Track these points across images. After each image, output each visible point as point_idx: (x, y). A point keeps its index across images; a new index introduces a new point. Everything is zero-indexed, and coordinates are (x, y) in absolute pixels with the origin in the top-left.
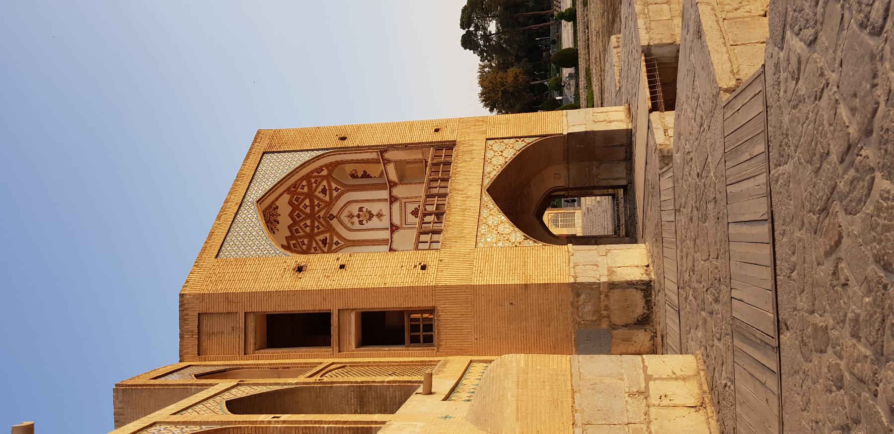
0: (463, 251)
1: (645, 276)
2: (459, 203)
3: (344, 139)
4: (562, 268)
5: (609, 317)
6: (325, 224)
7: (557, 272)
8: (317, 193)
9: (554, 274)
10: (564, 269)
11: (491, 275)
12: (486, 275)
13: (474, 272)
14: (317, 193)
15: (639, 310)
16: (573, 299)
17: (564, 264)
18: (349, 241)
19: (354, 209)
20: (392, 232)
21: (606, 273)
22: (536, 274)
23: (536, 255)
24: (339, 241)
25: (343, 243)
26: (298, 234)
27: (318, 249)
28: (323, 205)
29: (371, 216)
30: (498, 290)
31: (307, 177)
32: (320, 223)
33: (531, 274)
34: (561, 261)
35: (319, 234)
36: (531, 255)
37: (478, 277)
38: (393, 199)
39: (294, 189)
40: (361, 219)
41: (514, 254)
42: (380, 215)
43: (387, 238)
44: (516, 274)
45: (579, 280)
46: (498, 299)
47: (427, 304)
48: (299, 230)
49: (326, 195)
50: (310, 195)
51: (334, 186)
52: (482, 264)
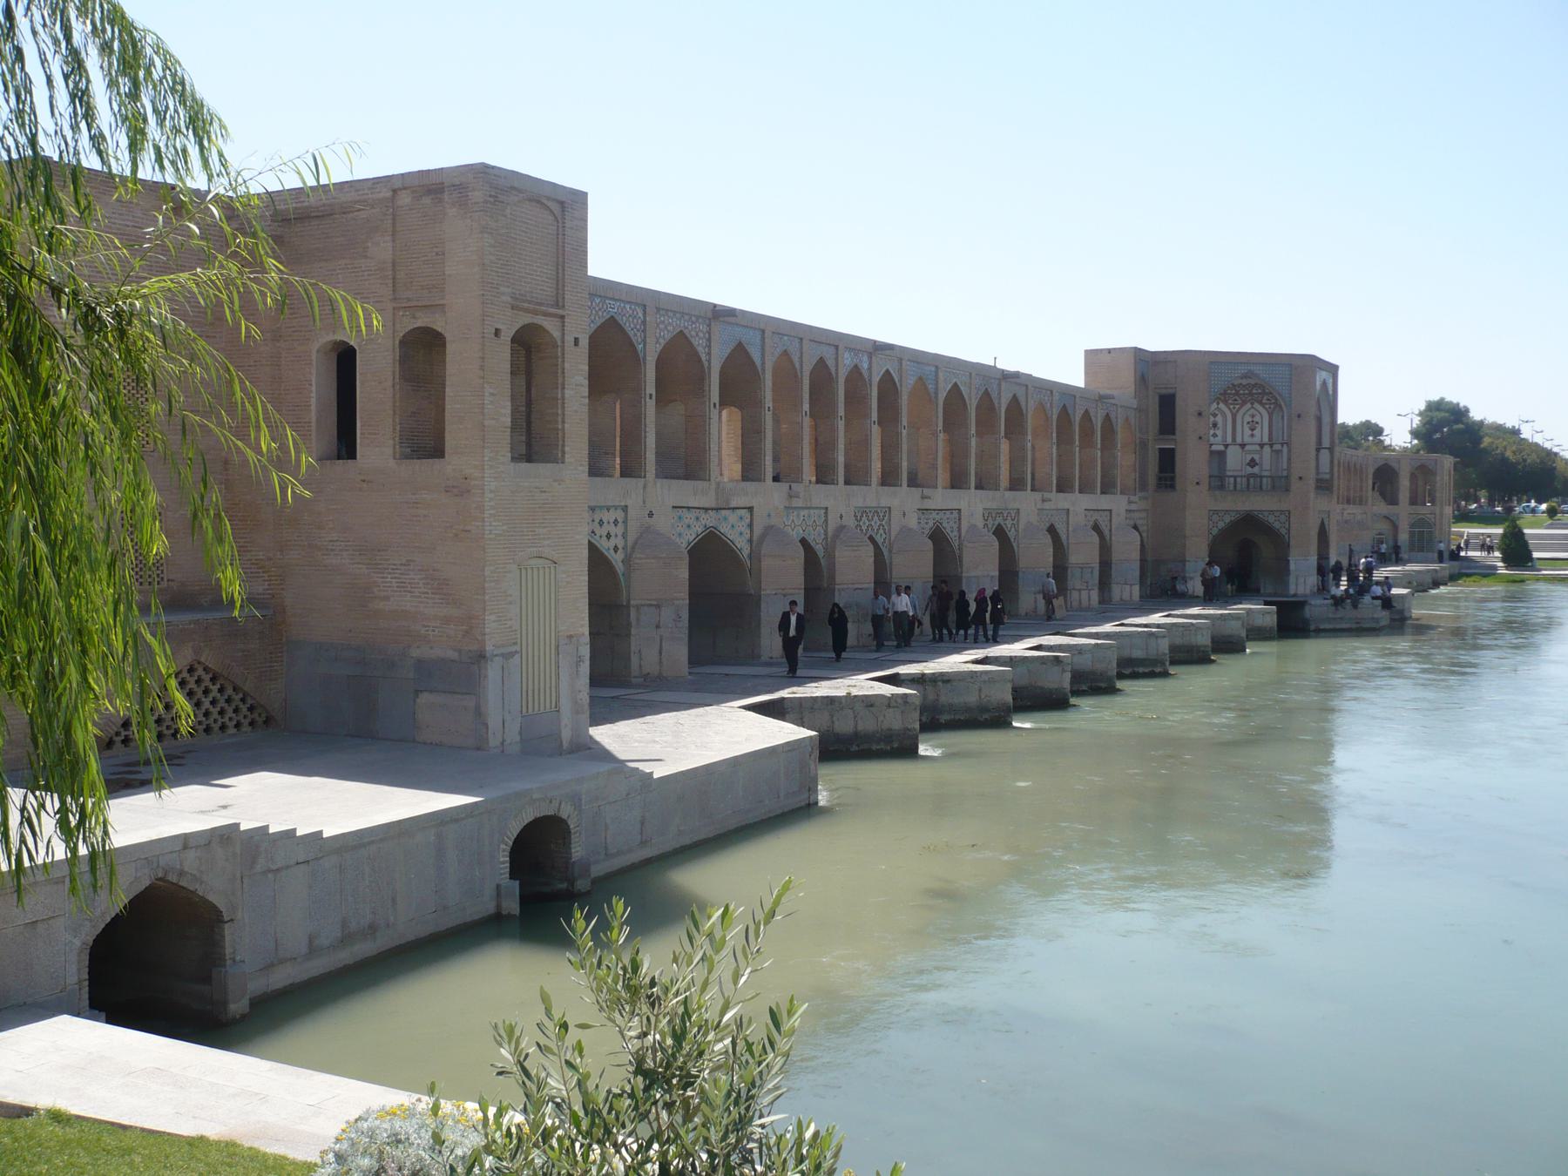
19: (1257, 419)
20: (1240, 445)
29: (1253, 430)
45: (1187, 563)
47: (1178, 486)
51: (1272, 406)
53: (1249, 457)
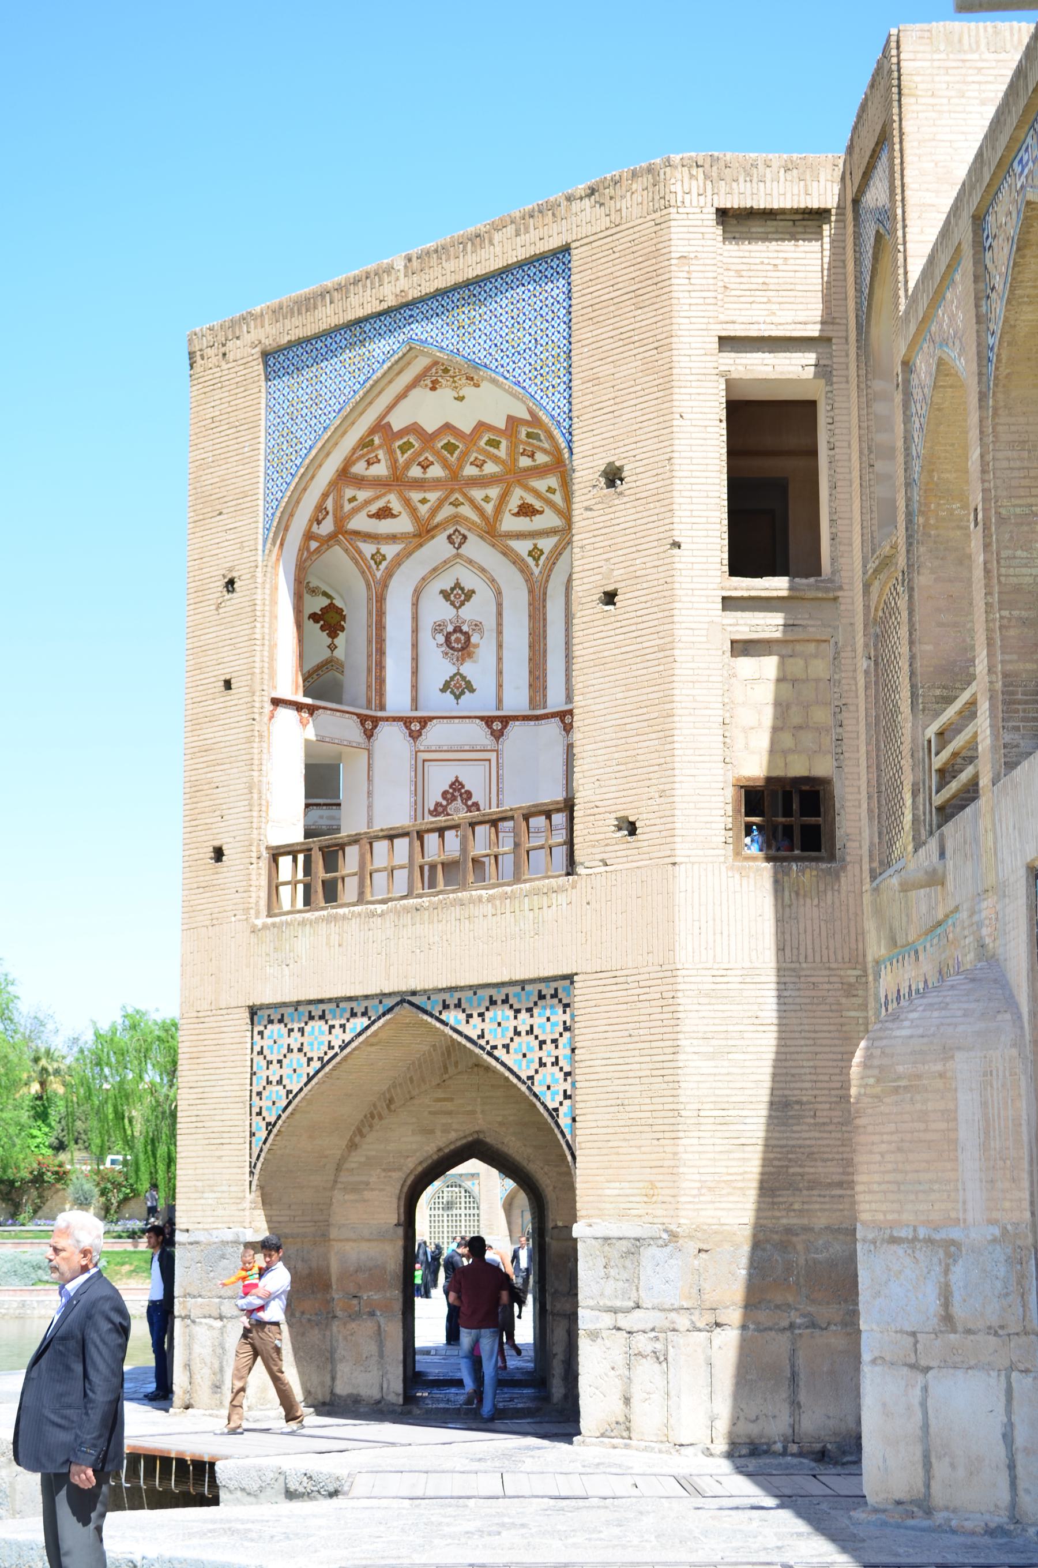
20: (407, 721)
24: (384, 564)
25: (379, 574)
43: (388, 707)
53: (439, 780)
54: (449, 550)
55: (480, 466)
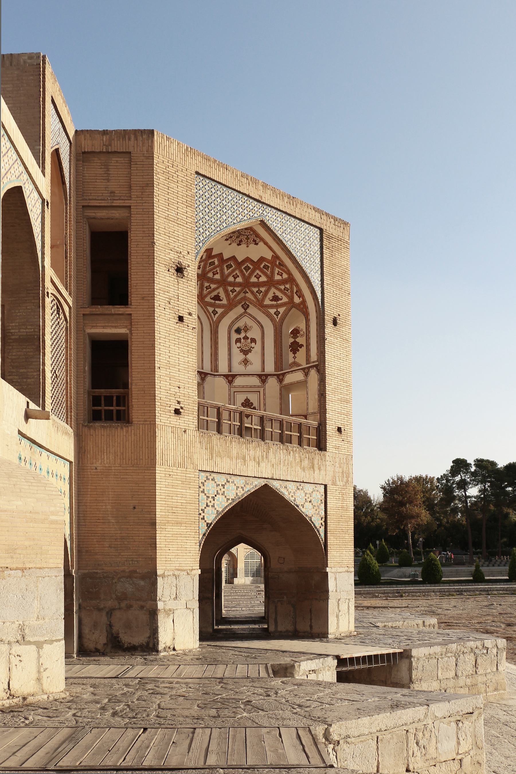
0: (195, 456)
1: (164, 646)
2: (252, 453)
3: (335, 322)
4: (173, 562)
5: (120, 609)
6: (238, 298)
7: (169, 557)
8: (273, 290)
9: (167, 554)
10: (172, 565)
11: (167, 486)
12: (167, 481)
13: (171, 468)
14: (273, 290)
15: (126, 639)
16: (140, 574)
17: (178, 565)
18: (217, 327)
20: (226, 376)
21: (167, 608)
22: (167, 535)
23: (189, 536)
24: (217, 315)
25: (215, 319)
26: (225, 268)
27: (208, 290)
28: (260, 296)
29: (246, 352)
30: (150, 494)
31: (291, 280)
32: (239, 293)
33: (167, 530)
34: (181, 562)
35: (226, 292)
36: (189, 531)
37: (164, 472)
38: (263, 377)
39: (278, 263)
40: (242, 340)
41: (191, 513)
42: (246, 362)
44: (168, 514)
45: (160, 580)
46: (139, 493)
48: (230, 269)
49: (271, 300)
50: (271, 283)
51: (281, 310)
52: (180, 477)
54: (243, 310)
55: (258, 278)
